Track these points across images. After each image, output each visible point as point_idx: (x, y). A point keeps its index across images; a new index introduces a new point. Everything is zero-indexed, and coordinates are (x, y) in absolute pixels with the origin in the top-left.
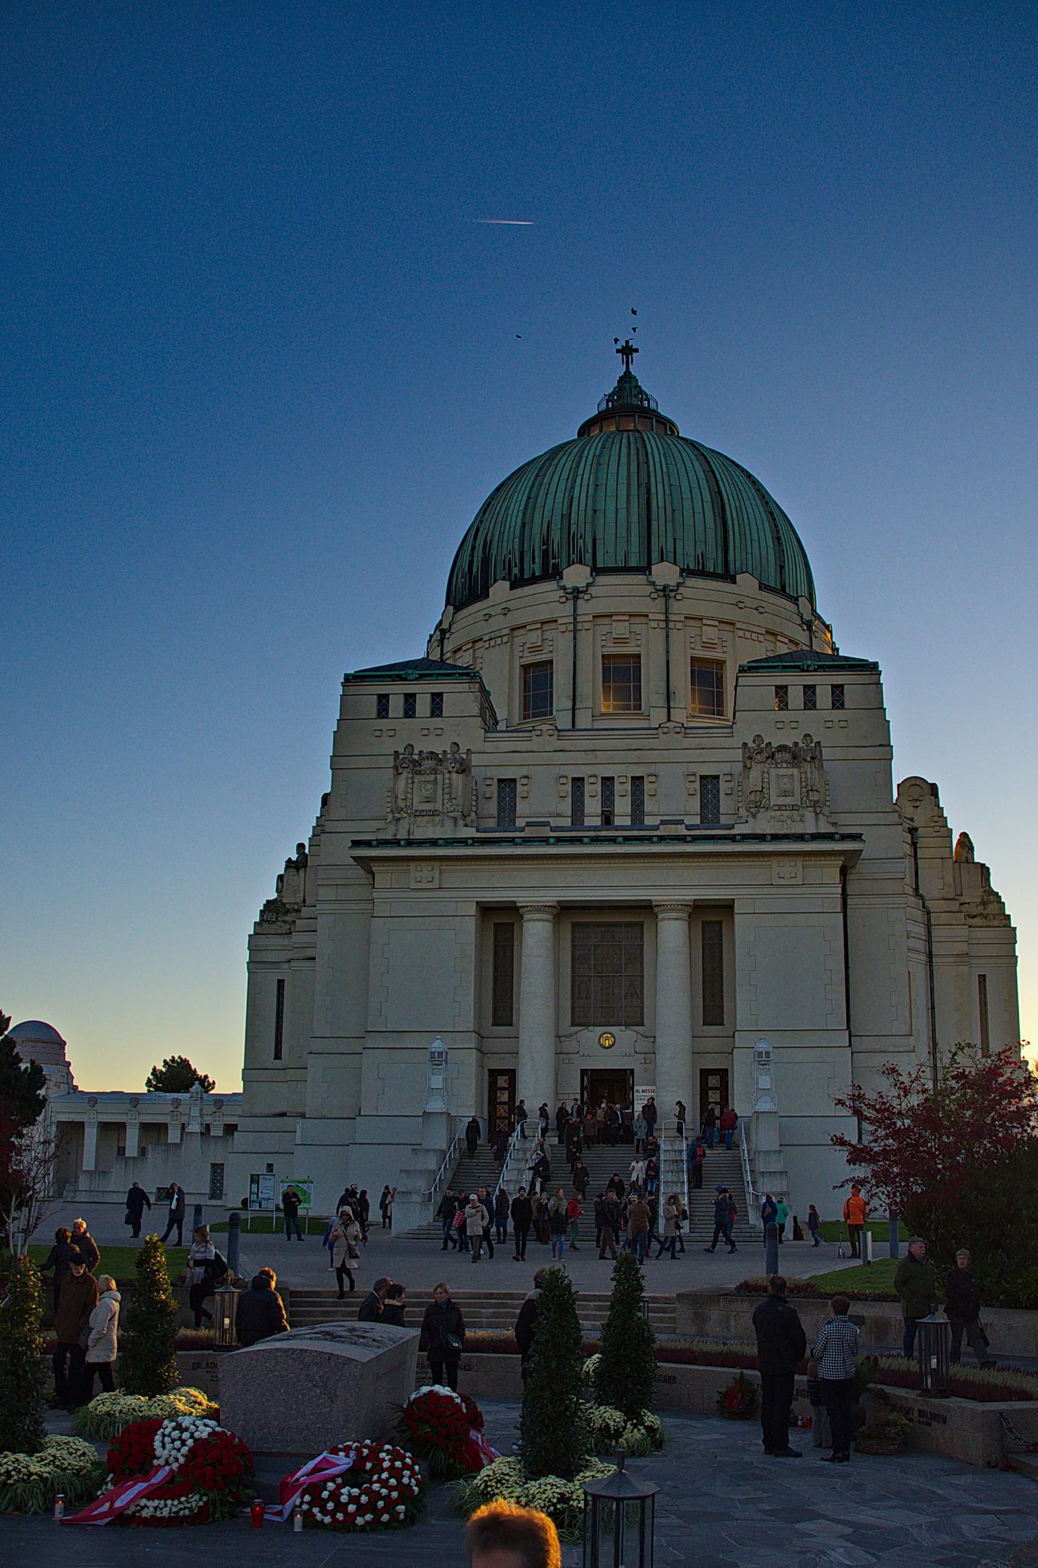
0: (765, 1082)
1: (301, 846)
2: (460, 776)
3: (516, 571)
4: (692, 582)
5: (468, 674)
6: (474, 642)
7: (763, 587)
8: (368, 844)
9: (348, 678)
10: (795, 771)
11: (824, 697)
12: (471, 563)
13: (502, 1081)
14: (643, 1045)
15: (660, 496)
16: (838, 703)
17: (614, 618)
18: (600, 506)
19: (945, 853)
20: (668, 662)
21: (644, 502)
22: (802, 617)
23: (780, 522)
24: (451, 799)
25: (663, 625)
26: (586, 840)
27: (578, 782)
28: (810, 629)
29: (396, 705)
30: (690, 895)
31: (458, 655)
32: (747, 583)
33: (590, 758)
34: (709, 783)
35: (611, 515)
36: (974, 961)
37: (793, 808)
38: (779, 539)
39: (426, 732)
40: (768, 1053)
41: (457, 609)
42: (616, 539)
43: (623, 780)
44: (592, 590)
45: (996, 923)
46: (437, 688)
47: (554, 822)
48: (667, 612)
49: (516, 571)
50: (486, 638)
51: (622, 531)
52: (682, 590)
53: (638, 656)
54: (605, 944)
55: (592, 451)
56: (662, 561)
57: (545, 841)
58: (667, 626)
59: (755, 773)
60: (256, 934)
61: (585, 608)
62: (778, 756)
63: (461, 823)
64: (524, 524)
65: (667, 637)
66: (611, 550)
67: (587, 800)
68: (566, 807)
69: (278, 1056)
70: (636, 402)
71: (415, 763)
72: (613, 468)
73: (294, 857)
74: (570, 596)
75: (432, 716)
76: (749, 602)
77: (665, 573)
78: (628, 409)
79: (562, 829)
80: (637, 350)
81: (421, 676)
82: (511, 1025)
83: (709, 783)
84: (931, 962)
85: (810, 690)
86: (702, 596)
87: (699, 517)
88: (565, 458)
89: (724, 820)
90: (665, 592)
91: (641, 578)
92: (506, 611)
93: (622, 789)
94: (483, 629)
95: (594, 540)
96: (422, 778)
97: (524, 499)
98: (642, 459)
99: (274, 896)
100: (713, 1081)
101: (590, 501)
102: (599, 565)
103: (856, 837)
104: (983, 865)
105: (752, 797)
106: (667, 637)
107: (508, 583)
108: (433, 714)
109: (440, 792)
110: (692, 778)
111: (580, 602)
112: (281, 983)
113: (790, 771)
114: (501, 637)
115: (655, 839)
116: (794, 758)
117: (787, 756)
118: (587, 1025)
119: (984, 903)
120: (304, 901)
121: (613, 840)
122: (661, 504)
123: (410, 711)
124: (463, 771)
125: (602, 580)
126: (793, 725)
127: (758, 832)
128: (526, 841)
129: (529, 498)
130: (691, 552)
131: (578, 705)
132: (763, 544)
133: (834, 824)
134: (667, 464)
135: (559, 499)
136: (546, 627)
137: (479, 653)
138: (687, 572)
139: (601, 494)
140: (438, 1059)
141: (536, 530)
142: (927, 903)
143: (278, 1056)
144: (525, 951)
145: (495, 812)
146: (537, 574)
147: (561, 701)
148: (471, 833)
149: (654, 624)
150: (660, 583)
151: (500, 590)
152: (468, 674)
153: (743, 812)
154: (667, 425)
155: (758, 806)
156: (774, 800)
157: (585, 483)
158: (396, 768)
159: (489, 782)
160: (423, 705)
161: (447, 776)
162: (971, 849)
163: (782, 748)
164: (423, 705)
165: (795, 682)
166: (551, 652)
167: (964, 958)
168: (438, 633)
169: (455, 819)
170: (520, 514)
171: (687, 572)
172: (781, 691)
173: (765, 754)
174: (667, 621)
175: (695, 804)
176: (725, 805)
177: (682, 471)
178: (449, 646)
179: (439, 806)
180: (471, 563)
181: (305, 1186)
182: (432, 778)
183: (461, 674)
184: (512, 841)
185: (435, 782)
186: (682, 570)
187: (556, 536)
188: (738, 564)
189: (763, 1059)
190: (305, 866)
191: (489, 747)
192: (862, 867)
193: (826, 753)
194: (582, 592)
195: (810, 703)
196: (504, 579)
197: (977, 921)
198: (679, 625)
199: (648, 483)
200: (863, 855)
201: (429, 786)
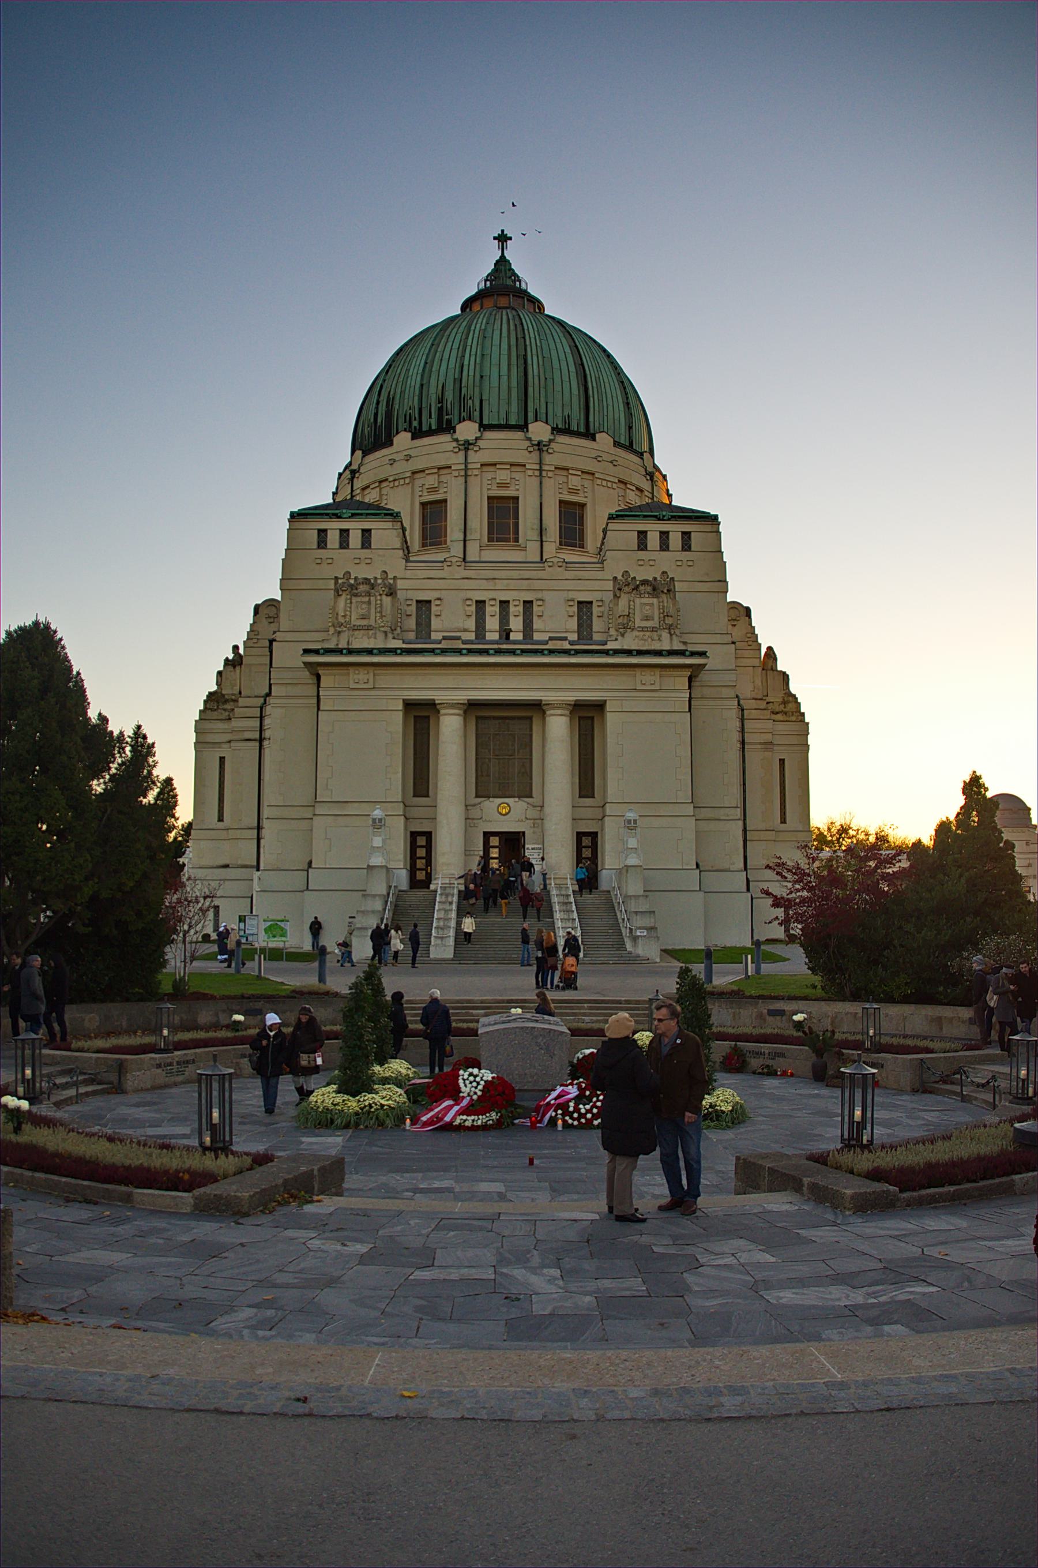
0: (632, 843)
1: (236, 648)
2: (389, 599)
3: (415, 424)
4: (562, 439)
5: (391, 515)
6: (380, 482)
7: (617, 444)
8: (316, 652)
9: (294, 516)
10: (655, 601)
11: (675, 540)
12: (376, 414)
13: (421, 841)
14: (532, 813)
15: (535, 367)
16: (686, 546)
18: (486, 372)
19: (756, 662)
20: (541, 504)
21: (522, 369)
23: (629, 390)
24: (382, 617)
25: (537, 473)
26: (491, 652)
27: (480, 604)
28: (652, 479)
29: (333, 538)
30: (572, 697)
31: (367, 491)
32: (604, 440)
33: (490, 585)
34: (585, 606)
36: (775, 748)
37: (653, 629)
38: (628, 404)
39: (358, 561)
40: (635, 821)
41: (365, 454)
43: (517, 603)
44: (480, 443)
45: (794, 718)
46: (367, 526)
47: (466, 636)
48: (540, 464)
49: (415, 424)
50: (391, 479)
52: (552, 445)
54: (503, 733)
55: (478, 326)
56: (536, 420)
57: (459, 652)
58: (541, 474)
59: (623, 601)
60: (201, 719)
61: (476, 458)
62: (641, 588)
63: (390, 636)
64: (422, 385)
65: (541, 483)
66: (495, 409)
68: (471, 623)
69: (221, 819)
70: (509, 282)
71: (351, 586)
72: (496, 341)
73: (231, 656)
74: (462, 447)
75: (363, 548)
76: (605, 457)
77: (539, 431)
78: (503, 290)
79: (471, 642)
80: (510, 238)
81: (353, 515)
82: (427, 796)
84: (743, 748)
85: (664, 535)
86: (569, 449)
87: (566, 385)
88: (455, 330)
89: (596, 637)
91: (520, 435)
92: (408, 458)
94: (388, 471)
95: (481, 401)
96: (359, 599)
97: (422, 365)
99: (214, 688)
101: (478, 367)
102: (485, 422)
103: (702, 654)
105: (620, 620)
106: (541, 483)
107: (410, 434)
108: (363, 547)
109: (373, 610)
110: (571, 603)
111: (470, 452)
112: (222, 760)
114: (404, 478)
115: (546, 652)
116: (654, 589)
117: (649, 589)
118: (489, 797)
119: (785, 703)
120: (240, 693)
121: (512, 652)
123: (344, 544)
124: (391, 594)
125: (488, 434)
126: (651, 563)
127: (625, 647)
128: (444, 651)
129: (426, 363)
130: (559, 414)
132: (616, 410)
133: (685, 643)
134: (540, 340)
135: (452, 365)
136: (442, 472)
137: (384, 491)
138: (556, 430)
139: (487, 364)
140: (378, 824)
141: (432, 390)
142: (742, 702)
143: (221, 819)
144: (442, 738)
145: (414, 627)
146: (433, 427)
147: (454, 533)
149: (530, 473)
150: (536, 439)
151: (403, 439)
152: (391, 515)
153: (612, 632)
154: (536, 304)
155: (626, 626)
156: (638, 623)
157: (473, 352)
158: (337, 591)
159: (409, 602)
160: (355, 539)
162: (775, 659)
163: (644, 582)
164: (355, 539)
165: (653, 529)
167: (769, 745)
168: (348, 472)
169: (386, 633)
171: (556, 430)
172: (642, 535)
173: (632, 587)
174: (541, 470)
175: (573, 624)
176: (597, 625)
177: (552, 345)
178: (358, 484)
179: (372, 622)
180: (376, 414)
181: (282, 924)
182: (366, 599)
183: (386, 515)
184: (432, 651)
185: (369, 602)
186: (553, 429)
187: (449, 396)
188: (597, 424)
189: (631, 826)
190: (241, 664)
191: (408, 574)
192: (703, 676)
195: (664, 546)
196: (405, 430)
197: (779, 717)
198: (550, 474)
199: (525, 355)
200: (707, 667)
201: (364, 606)
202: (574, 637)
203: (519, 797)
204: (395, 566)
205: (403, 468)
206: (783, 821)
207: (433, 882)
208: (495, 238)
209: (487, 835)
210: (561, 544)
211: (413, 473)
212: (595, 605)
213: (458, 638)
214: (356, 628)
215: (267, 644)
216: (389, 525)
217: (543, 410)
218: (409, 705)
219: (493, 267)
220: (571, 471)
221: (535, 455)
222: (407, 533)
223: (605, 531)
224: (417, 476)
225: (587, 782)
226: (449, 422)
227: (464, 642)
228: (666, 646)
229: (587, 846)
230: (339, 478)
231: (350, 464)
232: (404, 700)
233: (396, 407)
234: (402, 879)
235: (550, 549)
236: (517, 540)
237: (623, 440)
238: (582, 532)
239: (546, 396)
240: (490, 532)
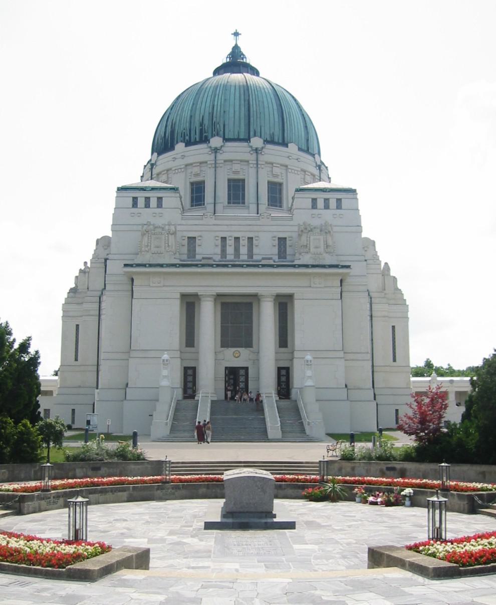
1: (85, 263)
3: (187, 138)
4: (269, 146)
7: (300, 149)
8: (131, 266)
10: (321, 237)
11: (333, 204)
13: (190, 372)
15: (254, 106)
17: (234, 162)
21: (247, 107)
22: (316, 163)
25: (255, 166)
27: (224, 239)
31: (160, 176)
32: (293, 148)
34: (282, 241)
35: (232, 115)
40: (311, 361)
41: (159, 154)
42: (234, 126)
46: (160, 195)
48: (257, 160)
51: (237, 123)
52: (264, 150)
53: (243, 180)
57: (211, 266)
61: (221, 157)
64: (191, 116)
69: (76, 360)
74: (213, 151)
77: (256, 142)
78: (235, 62)
80: (240, 34)
83: (282, 241)
84: (372, 319)
86: (273, 153)
87: (272, 116)
89: (288, 258)
91: (245, 144)
92: (183, 157)
93: (244, 242)
94: (171, 165)
102: (226, 137)
103: (348, 267)
104: (394, 277)
106: (257, 172)
107: (184, 144)
111: (218, 155)
113: (318, 237)
114: (181, 169)
117: (319, 230)
121: (241, 266)
122: (255, 109)
123: (147, 205)
125: (229, 144)
128: (203, 266)
130: (268, 133)
131: (216, 202)
137: (170, 176)
138: (266, 142)
142: (370, 294)
143: (76, 360)
146: (198, 140)
149: (251, 165)
150: (254, 146)
151: (180, 147)
156: (312, 250)
159: (184, 238)
160: (153, 202)
161: (167, 235)
164: (153, 202)
166: (204, 176)
168: (149, 165)
170: (189, 111)
171: (266, 142)
172: (314, 201)
174: (257, 164)
176: (289, 251)
178: (155, 171)
186: (264, 141)
187: (206, 122)
188: (289, 138)
191: (183, 222)
192: (349, 280)
193: (335, 229)
194: (219, 149)
196: (182, 141)
202: (276, 258)
205: (180, 163)
206: (394, 360)
207: (197, 395)
208: (232, 34)
209: (226, 368)
210: (268, 205)
211: (186, 165)
212: (287, 239)
213: (210, 258)
215: (103, 261)
216: (173, 195)
218: (183, 296)
219: (231, 50)
220: (274, 165)
221: (255, 155)
222: (182, 199)
223: (293, 198)
224: (188, 167)
225: (284, 339)
227: (214, 261)
229: (284, 377)
230: (144, 168)
231: (151, 160)
232: (180, 293)
233: (177, 128)
234: (179, 393)
235: (263, 207)
236: (244, 203)
237: (304, 147)
239: (260, 123)
240: (229, 199)
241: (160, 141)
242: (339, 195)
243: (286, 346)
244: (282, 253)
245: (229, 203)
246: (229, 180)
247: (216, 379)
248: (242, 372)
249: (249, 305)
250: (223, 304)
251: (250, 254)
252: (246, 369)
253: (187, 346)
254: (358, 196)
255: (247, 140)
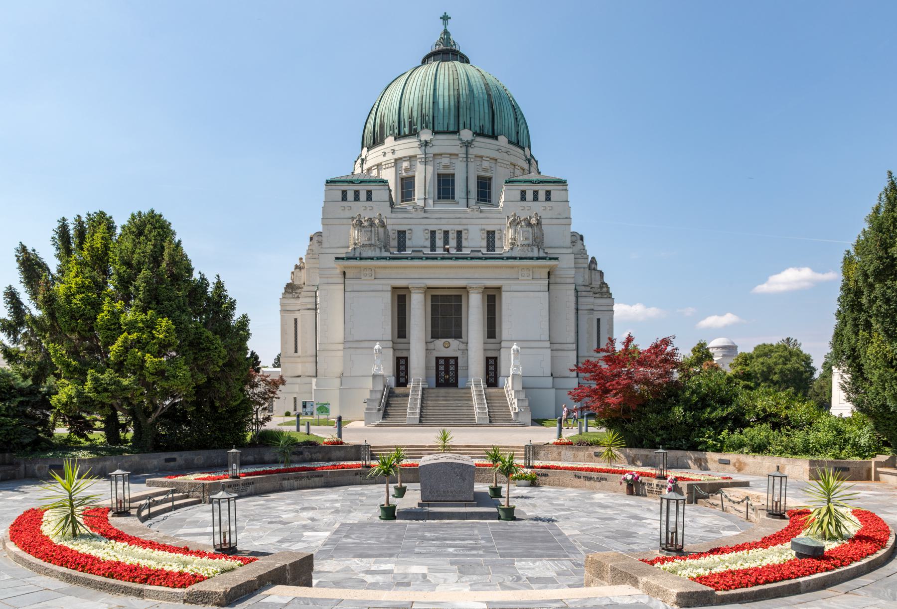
3: (396, 131)
7: (510, 142)
8: (342, 259)
9: (327, 182)
10: (530, 229)
11: (542, 195)
12: (374, 126)
13: (402, 362)
14: (462, 346)
16: (548, 198)
32: (503, 140)
33: (438, 221)
37: (528, 245)
41: (369, 149)
46: (369, 188)
48: (467, 154)
57: (421, 258)
61: (431, 150)
66: (441, 122)
67: (437, 240)
77: (466, 134)
86: (484, 146)
87: (482, 107)
90: (467, 145)
93: (452, 237)
94: (381, 159)
98: (455, 76)
100: (491, 362)
103: (556, 259)
107: (393, 138)
108: (368, 200)
118: (438, 338)
123: (357, 198)
130: (478, 125)
138: (476, 134)
141: (406, 111)
144: (412, 306)
148: (387, 254)
151: (390, 141)
160: (363, 195)
164: (363, 195)
165: (530, 189)
171: (476, 134)
172: (523, 193)
174: (467, 158)
176: (497, 243)
178: (366, 167)
180: (374, 126)
187: (415, 114)
191: (393, 215)
193: (543, 222)
202: (484, 251)
203: (455, 338)
204: (386, 210)
205: (390, 157)
209: (437, 359)
211: (396, 160)
213: (421, 251)
214: (364, 246)
217: (468, 122)
221: (464, 149)
225: (491, 330)
226: (415, 130)
228: (536, 254)
235: (472, 202)
236: (453, 198)
237: (514, 140)
238: (490, 193)
240: (439, 193)
241: (370, 135)
242: (548, 187)
243: (494, 337)
244: (491, 246)
245: (439, 198)
246: (439, 175)
247: (427, 368)
248: (452, 362)
249: (459, 297)
250: (434, 297)
251: (459, 247)
252: (456, 359)
253: (399, 337)
254: (568, 188)
255: (456, 132)
